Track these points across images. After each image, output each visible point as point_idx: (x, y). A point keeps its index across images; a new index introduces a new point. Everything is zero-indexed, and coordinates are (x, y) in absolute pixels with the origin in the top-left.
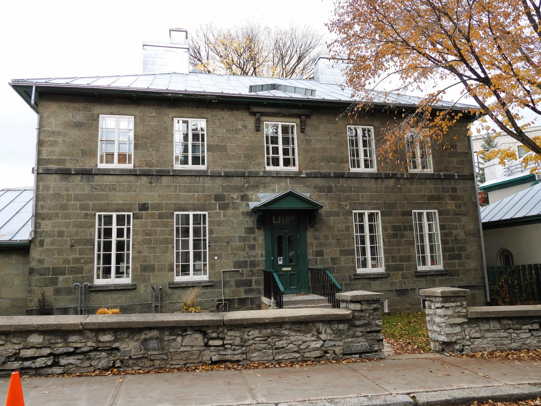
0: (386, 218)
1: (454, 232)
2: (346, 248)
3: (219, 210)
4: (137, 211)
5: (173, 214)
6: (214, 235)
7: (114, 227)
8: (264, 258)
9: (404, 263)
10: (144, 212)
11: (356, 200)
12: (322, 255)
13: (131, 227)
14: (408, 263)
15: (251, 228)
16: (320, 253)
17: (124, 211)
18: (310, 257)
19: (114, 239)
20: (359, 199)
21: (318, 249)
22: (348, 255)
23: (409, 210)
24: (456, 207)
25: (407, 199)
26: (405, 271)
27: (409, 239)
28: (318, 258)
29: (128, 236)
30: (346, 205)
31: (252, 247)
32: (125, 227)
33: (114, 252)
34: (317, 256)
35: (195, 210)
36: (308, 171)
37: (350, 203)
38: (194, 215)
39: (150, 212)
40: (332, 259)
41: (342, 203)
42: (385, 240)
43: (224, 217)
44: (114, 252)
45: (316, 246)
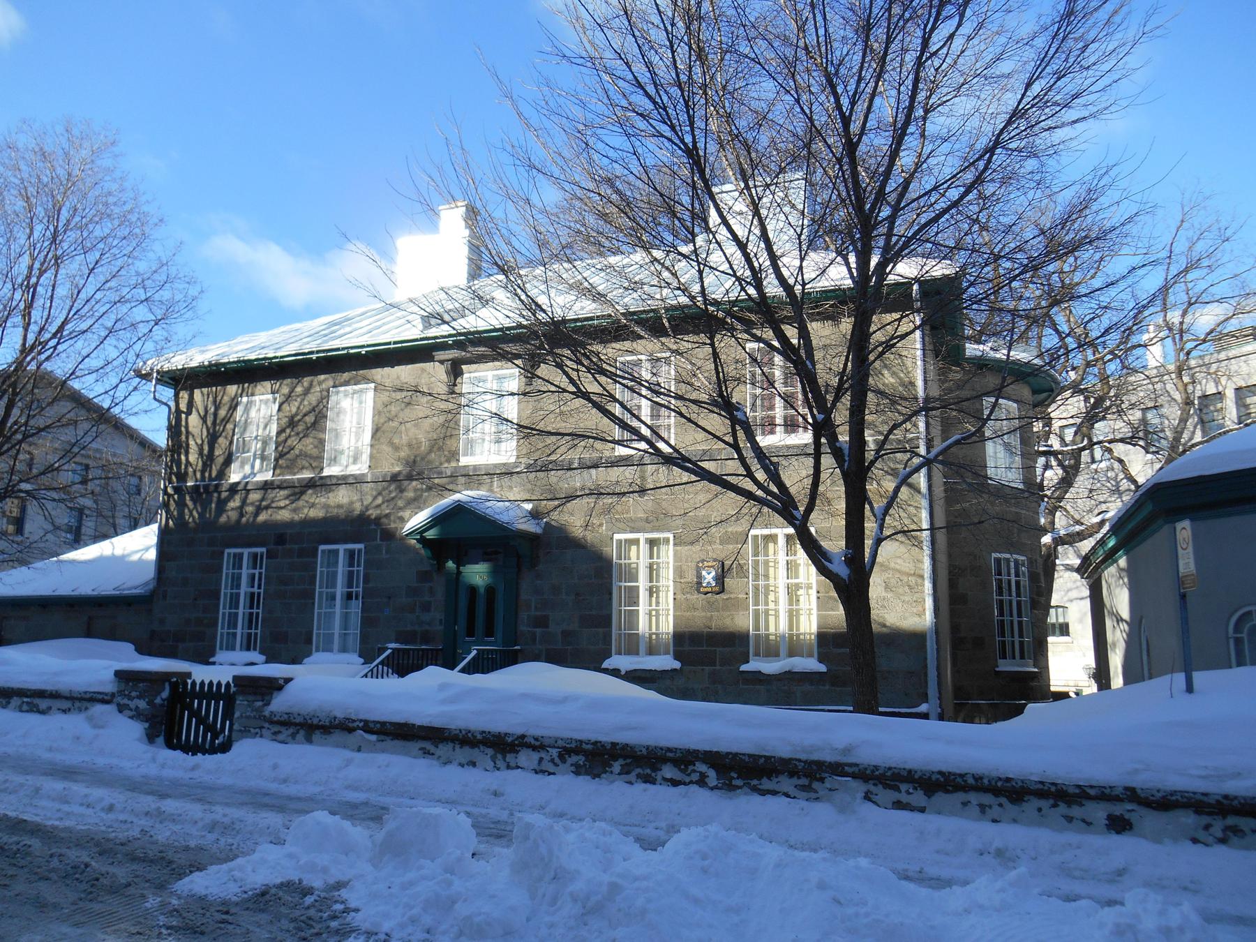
0: (684, 549)
2: (594, 612)
3: (381, 540)
4: (272, 547)
5: (317, 550)
6: (370, 585)
8: (442, 628)
9: (718, 649)
10: (280, 547)
12: (547, 626)
13: (263, 570)
14: (728, 649)
15: (426, 572)
16: (542, 622)
17: (256, 546)
18: (523, 628)
21: (538, 613)
22: (596, 627)
26: (718, 668)
27: (732, 596)
28: (538, 630)
29: (259, 587)
30: (601, 525)
31: (426, 607)
32: (257, 572)
34: (535, 627)
35: (346, 542)
38: (345, 550)
39: (288, 546)
40: (566, 634)
42: (678, 597)
43: (387, 553)
44: (241, 611)
45: (536, 607)
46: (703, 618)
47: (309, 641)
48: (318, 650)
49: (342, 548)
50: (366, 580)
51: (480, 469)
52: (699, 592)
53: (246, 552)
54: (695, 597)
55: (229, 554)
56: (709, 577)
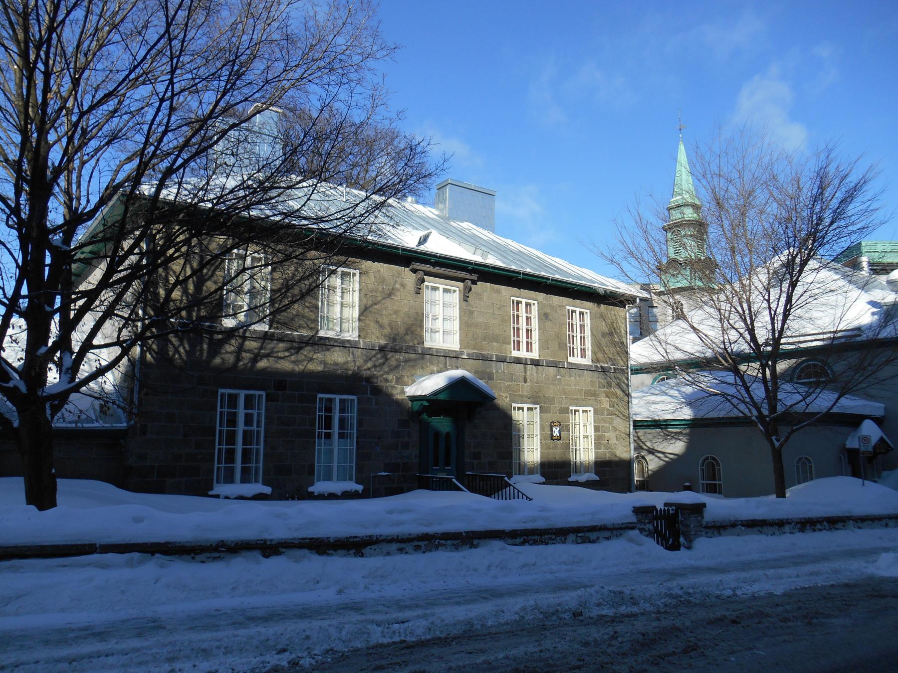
1: (607, 435)
7: (241, 412)
10: (280, 392)
11: (516, 392)
16: (477, 456)
17: (255, 389)
18: (467, 460)
19: (241, 427)
20: (519, 390)
23: (567, 406)
24: (610, 406)
25: (565, 394)
28: (476, 462)
30: (507, 397)
32: (255, 412)
33: (239, 447)
35: (342, 393)
36: (470, 351)
37: (510, 395)
41: (502, 394)
44: (239, 447)
46: (556, 455)
47: (311, 472)
48: (319, 480)
49: (337, 397)
50: (360, 423)
51: (440, 352)
52: (552, 439)
53: (242, 394)
54: (550, 441)
55: (223, 395)
56: (556, 433)
